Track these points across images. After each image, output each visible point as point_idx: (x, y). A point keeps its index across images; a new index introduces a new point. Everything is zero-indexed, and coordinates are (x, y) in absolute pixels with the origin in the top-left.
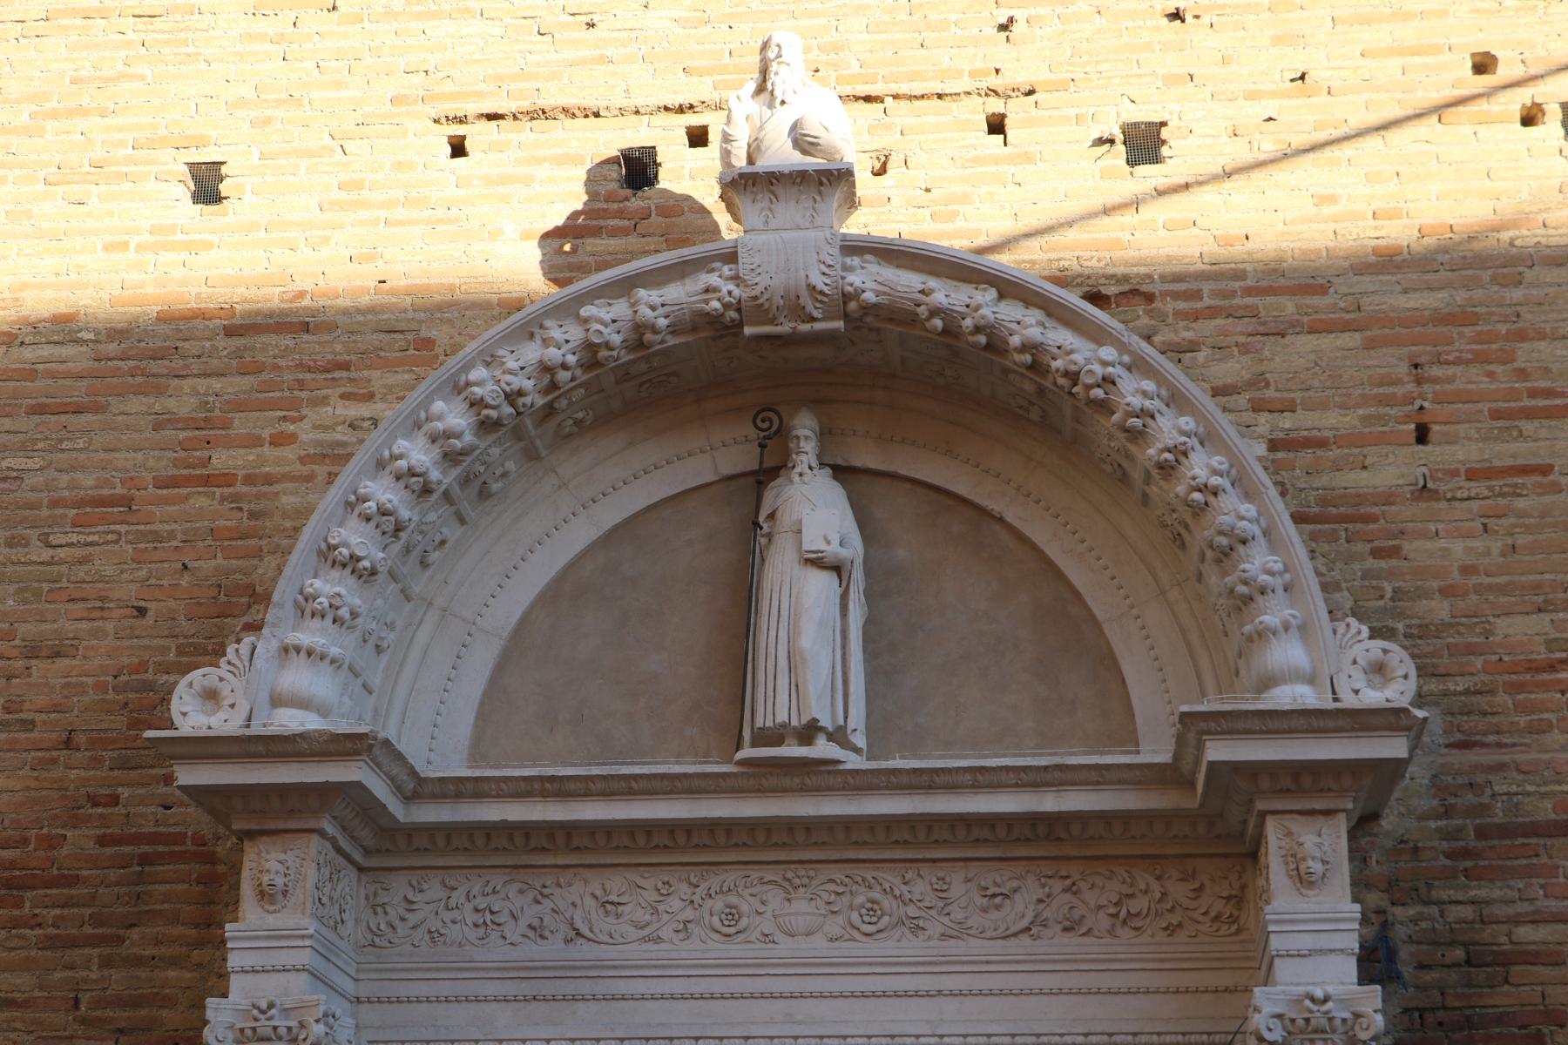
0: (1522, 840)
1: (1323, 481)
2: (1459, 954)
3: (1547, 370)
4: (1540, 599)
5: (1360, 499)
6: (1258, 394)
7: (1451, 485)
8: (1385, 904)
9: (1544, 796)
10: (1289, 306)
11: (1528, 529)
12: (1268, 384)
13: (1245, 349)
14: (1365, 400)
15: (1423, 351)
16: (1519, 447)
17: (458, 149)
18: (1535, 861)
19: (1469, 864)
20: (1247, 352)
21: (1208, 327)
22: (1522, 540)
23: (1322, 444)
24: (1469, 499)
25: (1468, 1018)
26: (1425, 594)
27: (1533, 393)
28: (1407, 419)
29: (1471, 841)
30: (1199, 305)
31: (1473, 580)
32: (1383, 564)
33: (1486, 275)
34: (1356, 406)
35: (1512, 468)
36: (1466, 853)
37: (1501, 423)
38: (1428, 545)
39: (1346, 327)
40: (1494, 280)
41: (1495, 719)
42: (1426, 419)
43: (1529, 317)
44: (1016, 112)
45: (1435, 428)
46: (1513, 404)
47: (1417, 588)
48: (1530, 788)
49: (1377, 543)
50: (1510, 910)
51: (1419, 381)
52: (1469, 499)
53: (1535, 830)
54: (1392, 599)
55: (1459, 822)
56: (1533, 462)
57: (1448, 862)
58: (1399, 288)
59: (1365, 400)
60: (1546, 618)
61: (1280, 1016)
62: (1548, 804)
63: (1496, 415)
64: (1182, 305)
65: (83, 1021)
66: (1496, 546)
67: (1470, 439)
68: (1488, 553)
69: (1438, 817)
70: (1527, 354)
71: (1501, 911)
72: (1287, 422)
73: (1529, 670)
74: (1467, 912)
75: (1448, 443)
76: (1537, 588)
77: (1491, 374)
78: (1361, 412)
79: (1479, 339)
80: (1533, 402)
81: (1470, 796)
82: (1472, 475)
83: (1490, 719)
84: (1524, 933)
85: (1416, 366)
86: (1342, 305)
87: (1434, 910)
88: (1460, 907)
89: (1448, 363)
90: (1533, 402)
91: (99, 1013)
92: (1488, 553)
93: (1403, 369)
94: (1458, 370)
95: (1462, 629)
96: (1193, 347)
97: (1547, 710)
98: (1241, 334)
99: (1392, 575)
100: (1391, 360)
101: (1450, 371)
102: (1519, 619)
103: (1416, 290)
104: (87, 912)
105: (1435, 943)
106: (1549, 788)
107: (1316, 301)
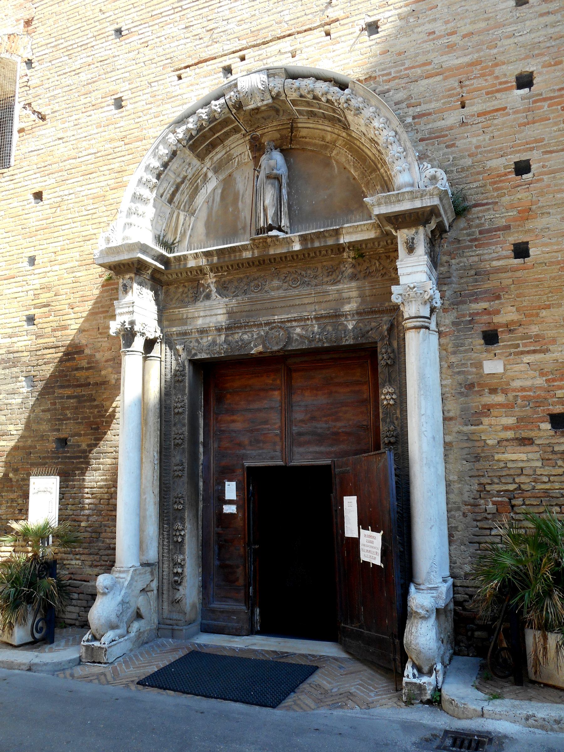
0: (494, 233)
1: (430, 126)
2: (473, 272)
3: (505, 75)
4: (503, 152)
5: (442, 130)
6: (409, 102)
7: (472, 120)
8: (448, 260)
9: (502, 217)
10: (419, 71)
11: (498, 130)
12: (412, 98)
13: (404, 88)
14: (444, 97)
15: (463, 77)
16: (496, 102)
17: (180, 78)
18: (499, 239)
19: (476, 243)
20: (405, 89)
21: (392, 84)
22: (496, 134)
23: (430, 114)
24: (478, 123)
25: (476, 292)
26: (463, 157)
27: (501, 83)
28: (458, 100)
29: (477, 235)
30: (390, 77)
31: (479, 150)
32: (450, 150)
33: (485, 47)
34: (441, 99)
35: (492, 110)
36: (476, 240)
37: (490, 96)
38: (465, 141)
39: (438, 74)
40: (487, 48)
41: (487, 195)
42: (464, 99)
43: (499, 58)
44: (332, 28)
45: (467, 102)
46: (494, 89)
47: (461, 156)
48: (497, 216)
49: (447, 143)
50: (490, 257)
51: (461, 87)
52: (478, 123)
53: (499, 229)
54: (452, 161)
55: (474, 230)
56: (500, 107)
57: (470, 243)
58: (455, 57)
59: (444, 97)
60: (504, 158)
61: (401, 295)
62: (504, 220)
63: (487, 93)
64: (385, 78)
65: (100, 334)
66: (487, 137)
67: (479, 103)
68: (484, 140)
69: (466, 229)
70: (498, 71)
71: (487, 257)
72: (418, 109)
73: (498, 176)
74: (476, 259)
75: (472, 106)
76: (501, 149)
77: (486, 80)
78: (442, 101)
79: (482, 69)
80: (501, 87)
81: (477, 221)
82: (479, 115)
83: (484, 195)
84: (495, 263)
85: (461, 82)
86: (436, 67)
87: (465, 259)
88: (473, 258)
89: (471, 79)
90: (501, 87)
91: (104, 331)
92: (484, 140)
93: (456, 84)
94: (475, 81)
95: (475, 167)
96: (388, 91)
97: (504, 189)
98: (404, 83)
99: (452, 153)
100: (453, 82)
101: (472, 82)
102: (495, 161)
103: (460, 57)
104: (100, 305)
105: (465, 270)
106: (504, 215)
107: (427, 68)
